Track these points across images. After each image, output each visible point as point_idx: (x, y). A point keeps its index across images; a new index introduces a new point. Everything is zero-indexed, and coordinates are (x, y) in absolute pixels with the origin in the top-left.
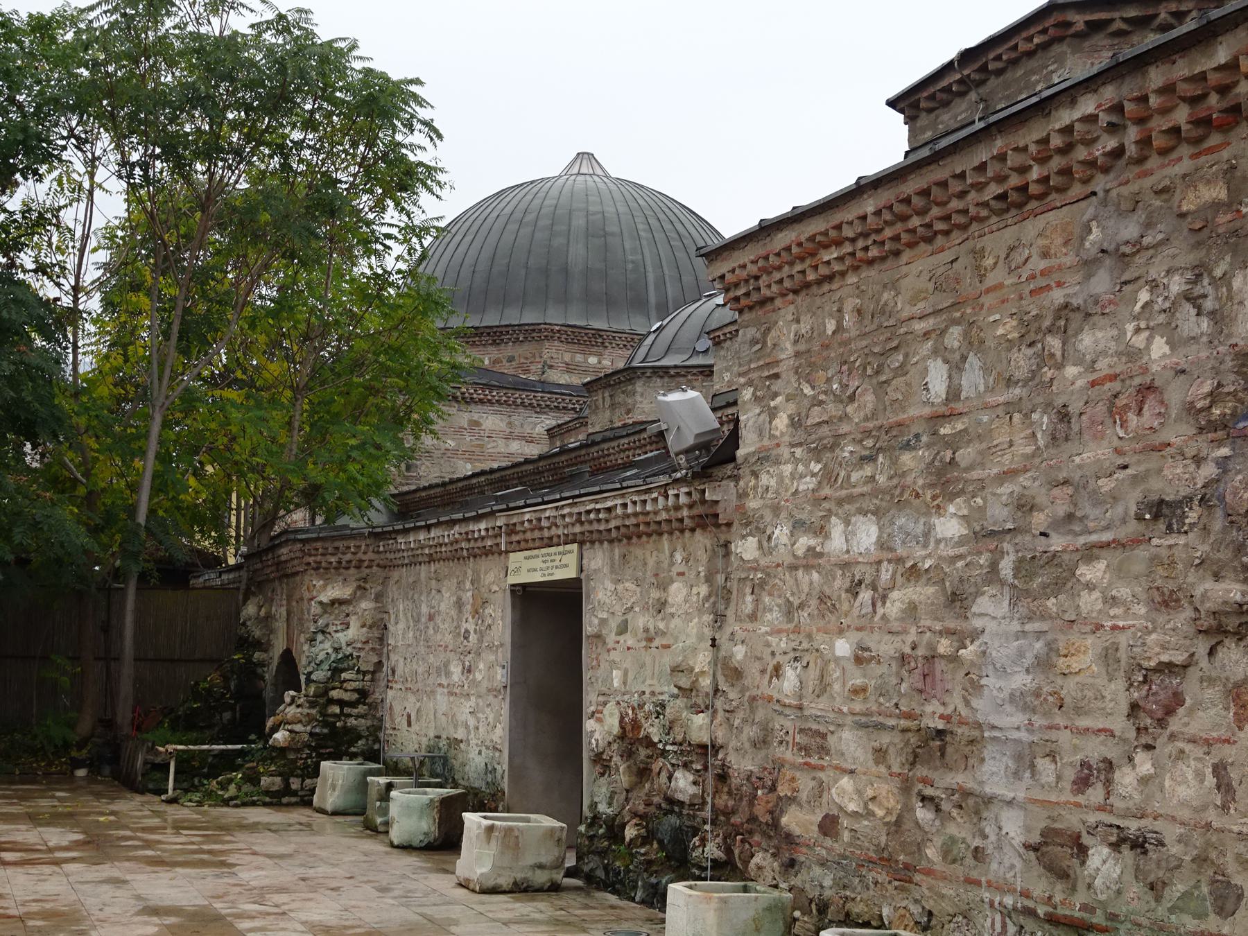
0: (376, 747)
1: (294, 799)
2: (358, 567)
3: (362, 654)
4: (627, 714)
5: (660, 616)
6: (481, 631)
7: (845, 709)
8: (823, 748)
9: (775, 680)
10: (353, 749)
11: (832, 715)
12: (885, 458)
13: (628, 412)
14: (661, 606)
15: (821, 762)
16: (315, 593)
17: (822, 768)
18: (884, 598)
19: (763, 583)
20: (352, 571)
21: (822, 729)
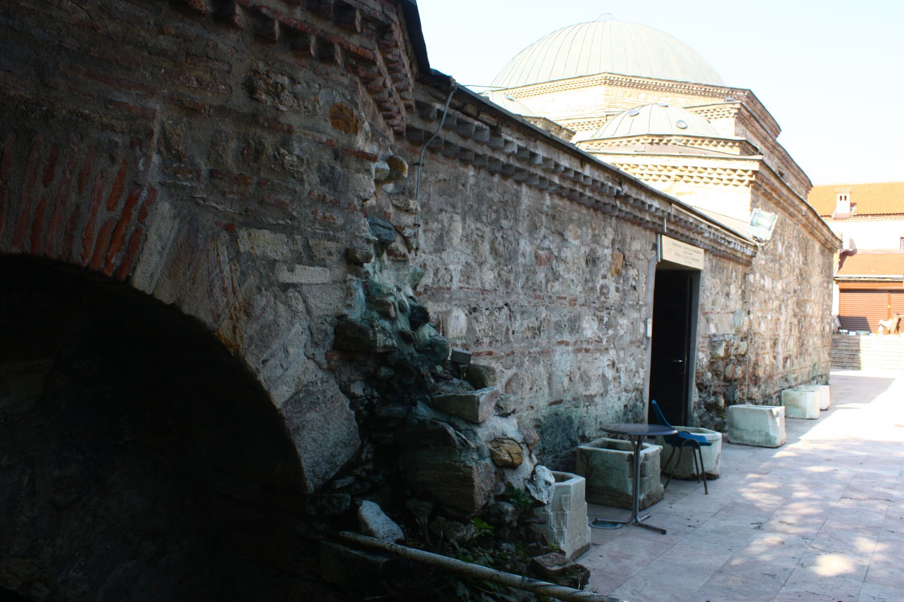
6: (624, 290)
14: (728, 295)
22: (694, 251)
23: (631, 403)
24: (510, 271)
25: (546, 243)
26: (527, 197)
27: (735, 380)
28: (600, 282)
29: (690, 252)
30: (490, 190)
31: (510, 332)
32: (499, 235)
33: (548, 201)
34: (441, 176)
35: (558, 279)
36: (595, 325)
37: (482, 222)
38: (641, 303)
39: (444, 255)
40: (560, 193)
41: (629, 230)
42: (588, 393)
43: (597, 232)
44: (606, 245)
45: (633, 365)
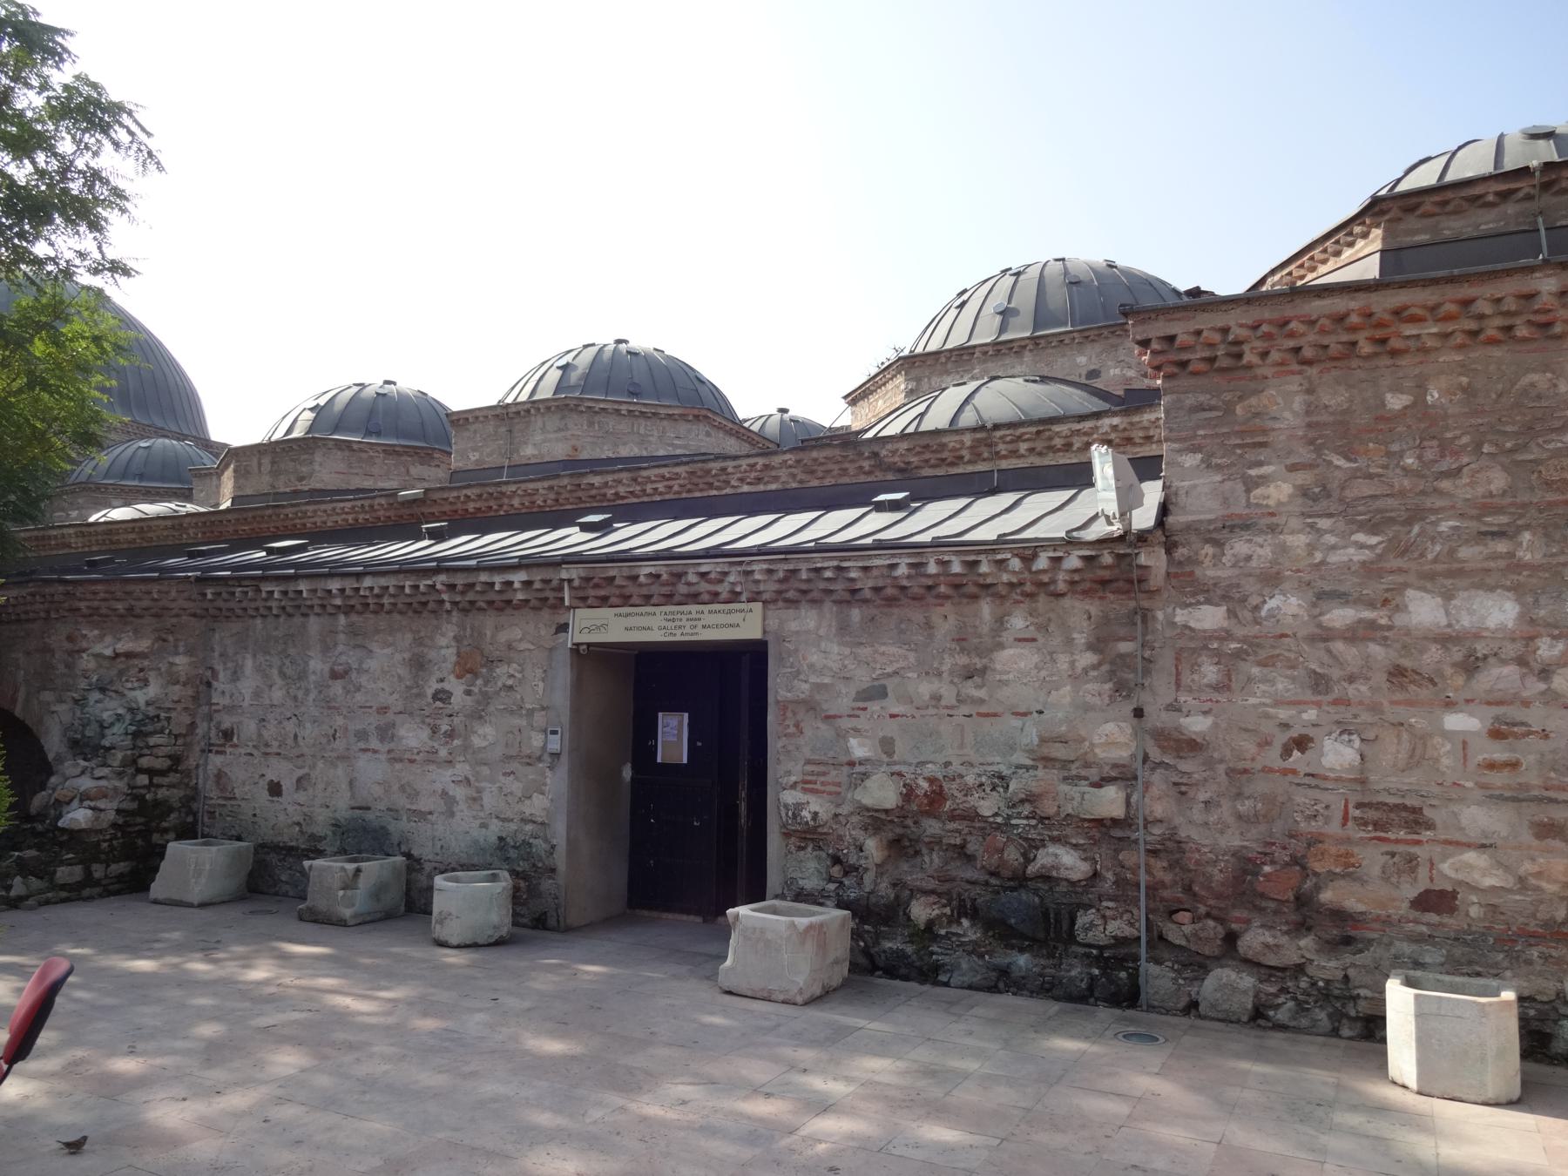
0: (190, 819)
1: (97, 890)
2: (157, 616)
3: (173, 715)
4: (918, 786)
5: (970, 682)
6: (485, 695)
7: (1469, 784)
8: (1417, 822)
9: (1296, 754)
10: (165, 824)
11: (1436, 790)
12: (1534, 535)
13: (301, 479)
15: (1415, 837)
16: (84, 644)
17: (1418, 842)
18: (1545, 673)
19: (1238, 655)
20: (147, 620)
21: (1408, 802)
22: (710, 612)
23: (520, 837)
24: (299, 688)
25: (343, 658)
26: (314, 624)
27: (1046, 878)
28: (432, 686)
29: (694, 616)
30: (276, 629)
31: (300, 739)
32: (287, 662)
33: (342, 619)
34: (234, 631)
35: (359, 690)
36: (425, 734)
37: (269, 654)
38: (528, 706)
39: (238, 684)
40: (348, 610)
41: (488, 622)
42: (414, 808)
43: (422, 634)
44: (444, 644)
45: (516, 787)
